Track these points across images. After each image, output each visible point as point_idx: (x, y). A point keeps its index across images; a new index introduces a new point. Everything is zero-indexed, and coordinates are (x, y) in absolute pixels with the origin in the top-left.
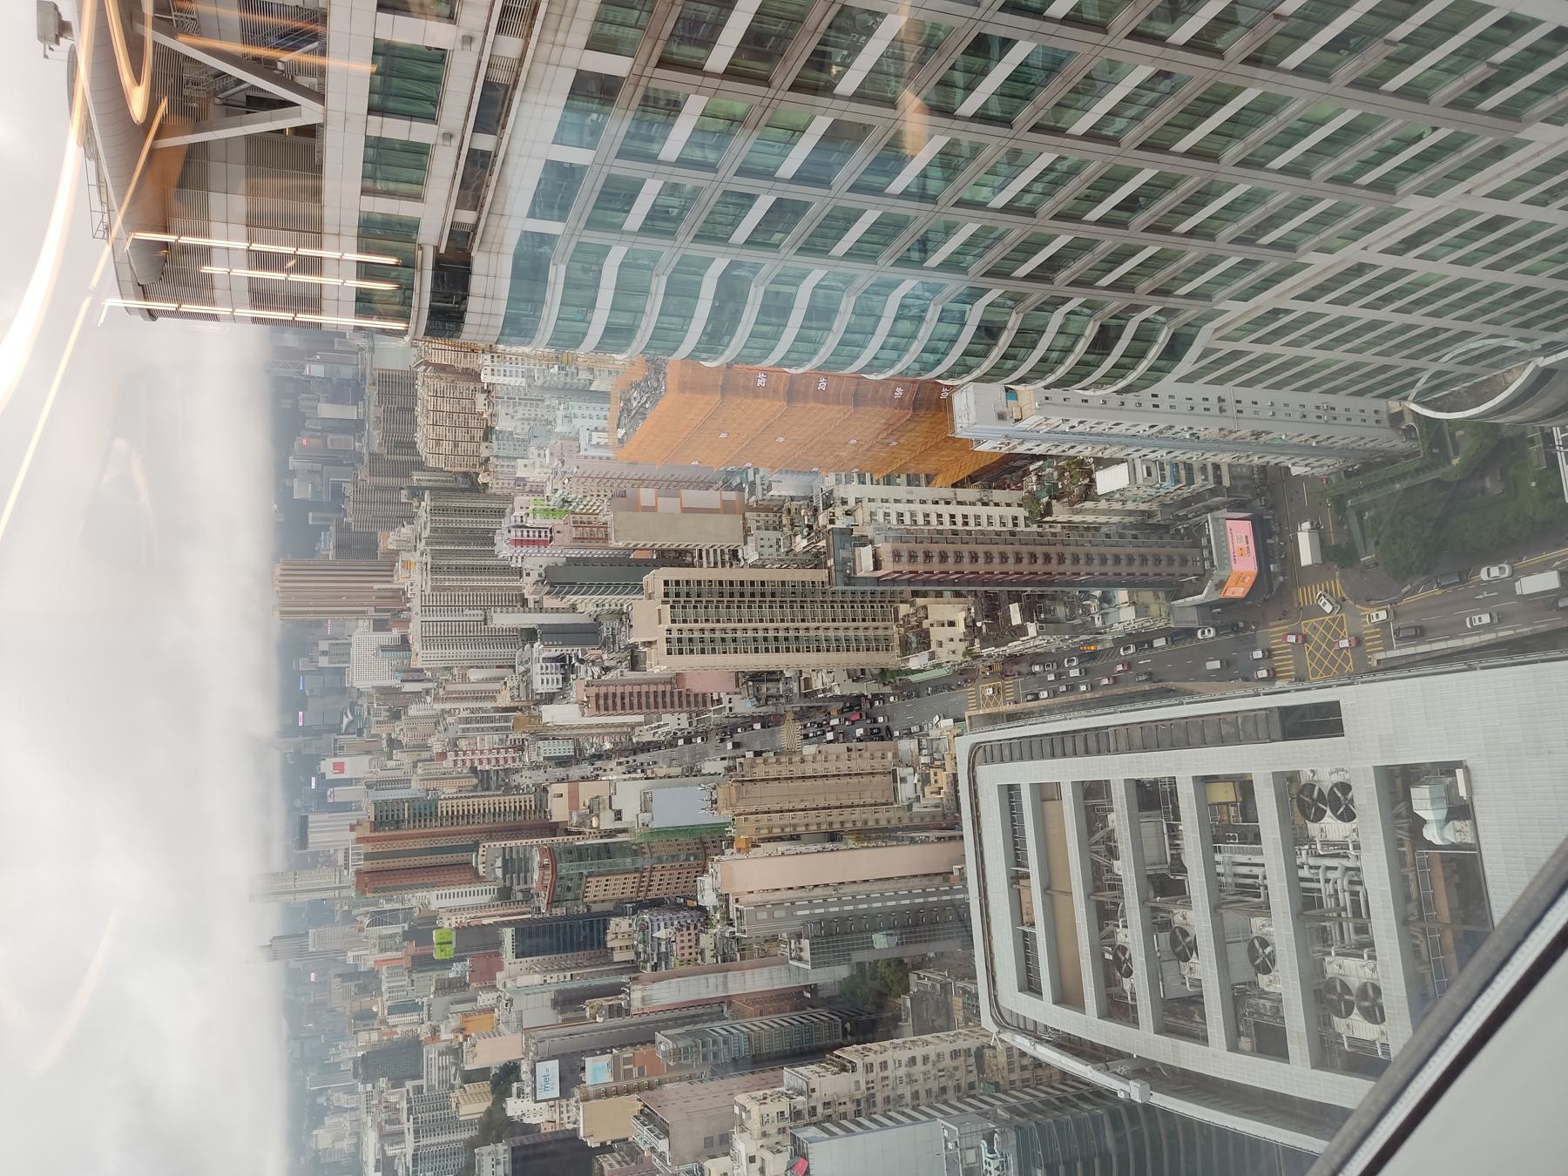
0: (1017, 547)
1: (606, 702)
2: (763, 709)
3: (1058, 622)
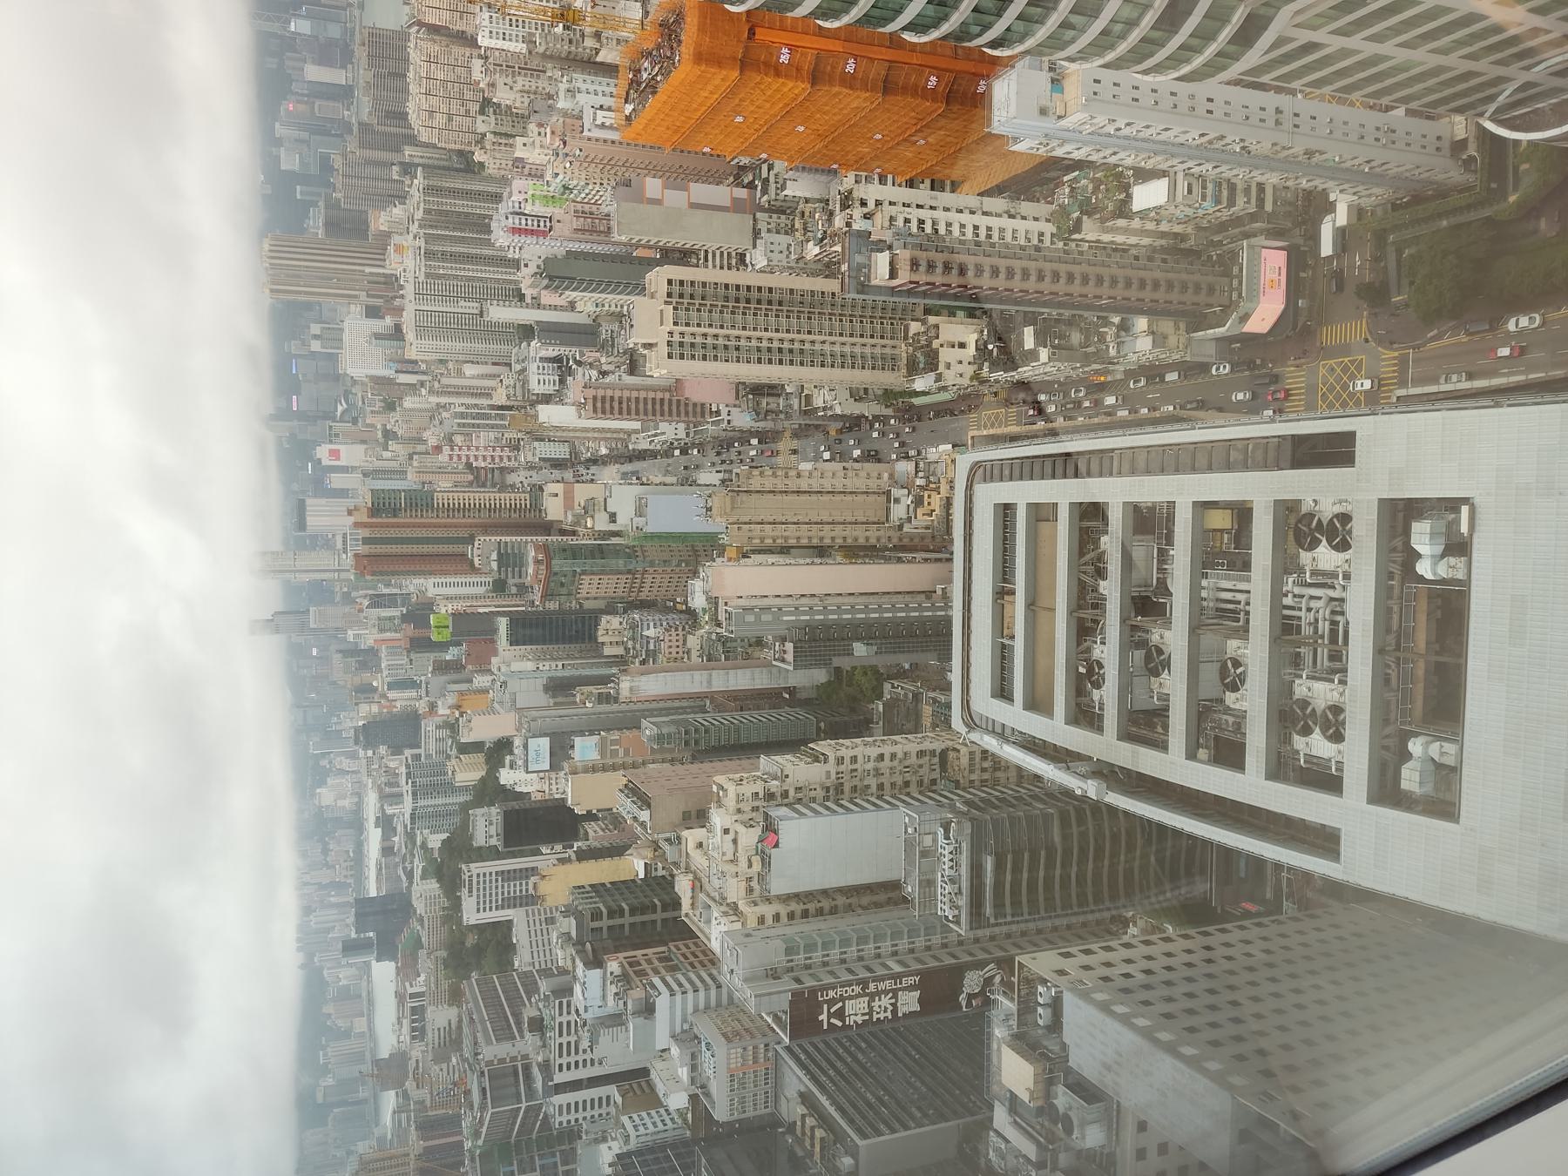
0: (1041, 264)
1: (603, 405)
2: (761, 424)
3: (1070, 348)
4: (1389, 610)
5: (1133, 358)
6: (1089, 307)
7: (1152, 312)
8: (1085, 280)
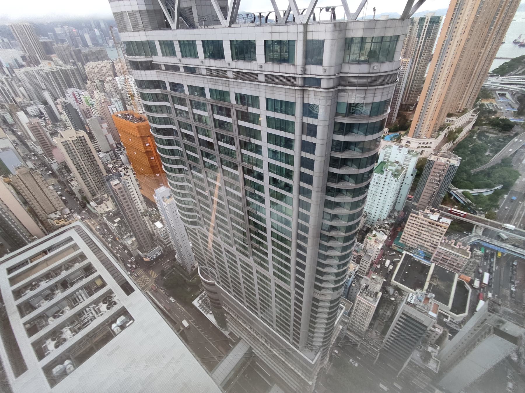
0: (135, 213)
1: (35, 129)
2: (57, 172)
3: (120, 229)
4: (99, 328)
5: (126, 242)
6: (131, 227)
7: (137, 240)
8: (136, 223)
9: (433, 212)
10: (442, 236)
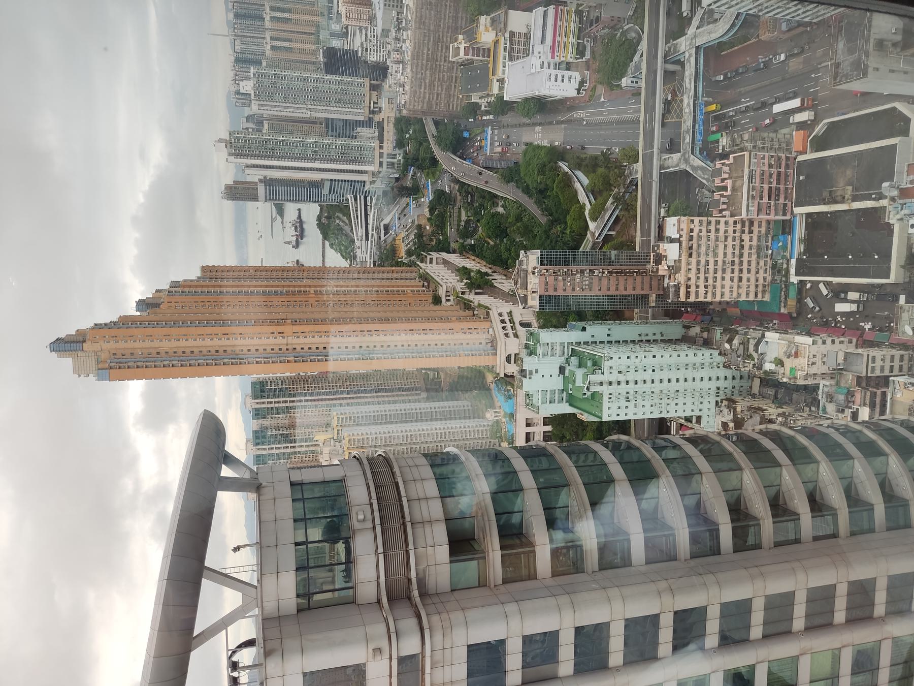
9: (659, 259)
10: (713, 220)
